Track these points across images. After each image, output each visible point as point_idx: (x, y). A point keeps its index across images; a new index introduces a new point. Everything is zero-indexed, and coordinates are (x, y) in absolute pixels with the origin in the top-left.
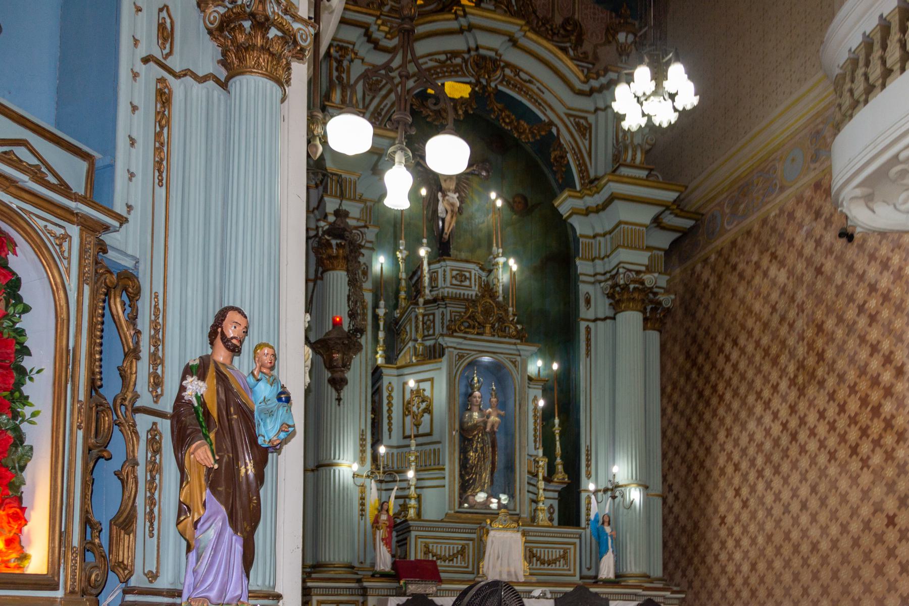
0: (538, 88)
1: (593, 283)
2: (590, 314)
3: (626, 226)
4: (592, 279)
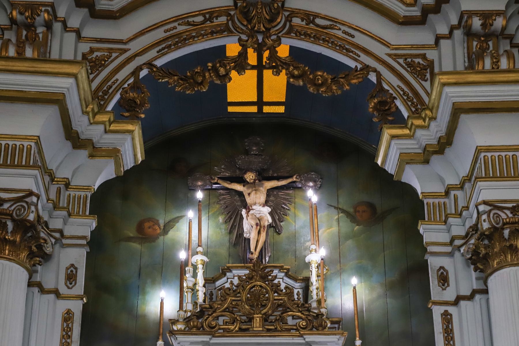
0: (345, 32)
1: (451, 255)
2: (450, 295)
3: (489, 155)
4: (449, 249)
